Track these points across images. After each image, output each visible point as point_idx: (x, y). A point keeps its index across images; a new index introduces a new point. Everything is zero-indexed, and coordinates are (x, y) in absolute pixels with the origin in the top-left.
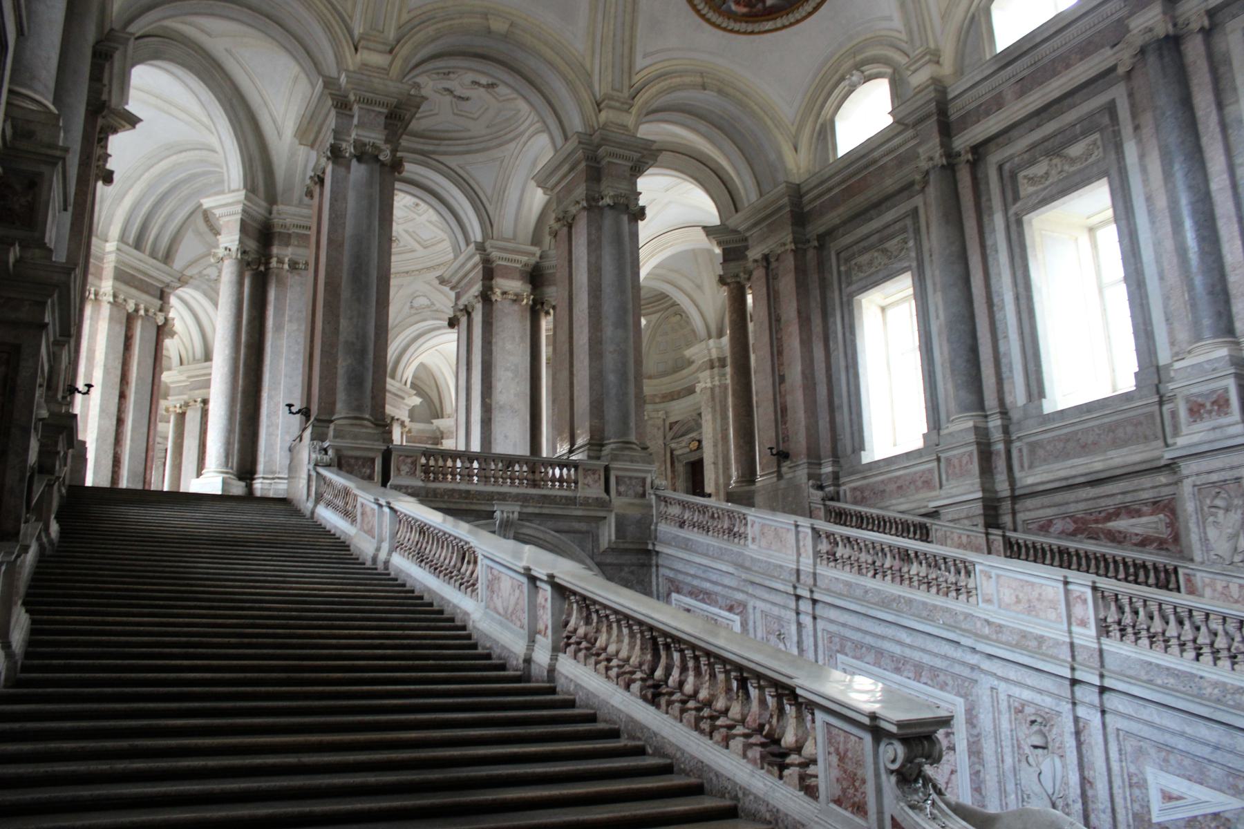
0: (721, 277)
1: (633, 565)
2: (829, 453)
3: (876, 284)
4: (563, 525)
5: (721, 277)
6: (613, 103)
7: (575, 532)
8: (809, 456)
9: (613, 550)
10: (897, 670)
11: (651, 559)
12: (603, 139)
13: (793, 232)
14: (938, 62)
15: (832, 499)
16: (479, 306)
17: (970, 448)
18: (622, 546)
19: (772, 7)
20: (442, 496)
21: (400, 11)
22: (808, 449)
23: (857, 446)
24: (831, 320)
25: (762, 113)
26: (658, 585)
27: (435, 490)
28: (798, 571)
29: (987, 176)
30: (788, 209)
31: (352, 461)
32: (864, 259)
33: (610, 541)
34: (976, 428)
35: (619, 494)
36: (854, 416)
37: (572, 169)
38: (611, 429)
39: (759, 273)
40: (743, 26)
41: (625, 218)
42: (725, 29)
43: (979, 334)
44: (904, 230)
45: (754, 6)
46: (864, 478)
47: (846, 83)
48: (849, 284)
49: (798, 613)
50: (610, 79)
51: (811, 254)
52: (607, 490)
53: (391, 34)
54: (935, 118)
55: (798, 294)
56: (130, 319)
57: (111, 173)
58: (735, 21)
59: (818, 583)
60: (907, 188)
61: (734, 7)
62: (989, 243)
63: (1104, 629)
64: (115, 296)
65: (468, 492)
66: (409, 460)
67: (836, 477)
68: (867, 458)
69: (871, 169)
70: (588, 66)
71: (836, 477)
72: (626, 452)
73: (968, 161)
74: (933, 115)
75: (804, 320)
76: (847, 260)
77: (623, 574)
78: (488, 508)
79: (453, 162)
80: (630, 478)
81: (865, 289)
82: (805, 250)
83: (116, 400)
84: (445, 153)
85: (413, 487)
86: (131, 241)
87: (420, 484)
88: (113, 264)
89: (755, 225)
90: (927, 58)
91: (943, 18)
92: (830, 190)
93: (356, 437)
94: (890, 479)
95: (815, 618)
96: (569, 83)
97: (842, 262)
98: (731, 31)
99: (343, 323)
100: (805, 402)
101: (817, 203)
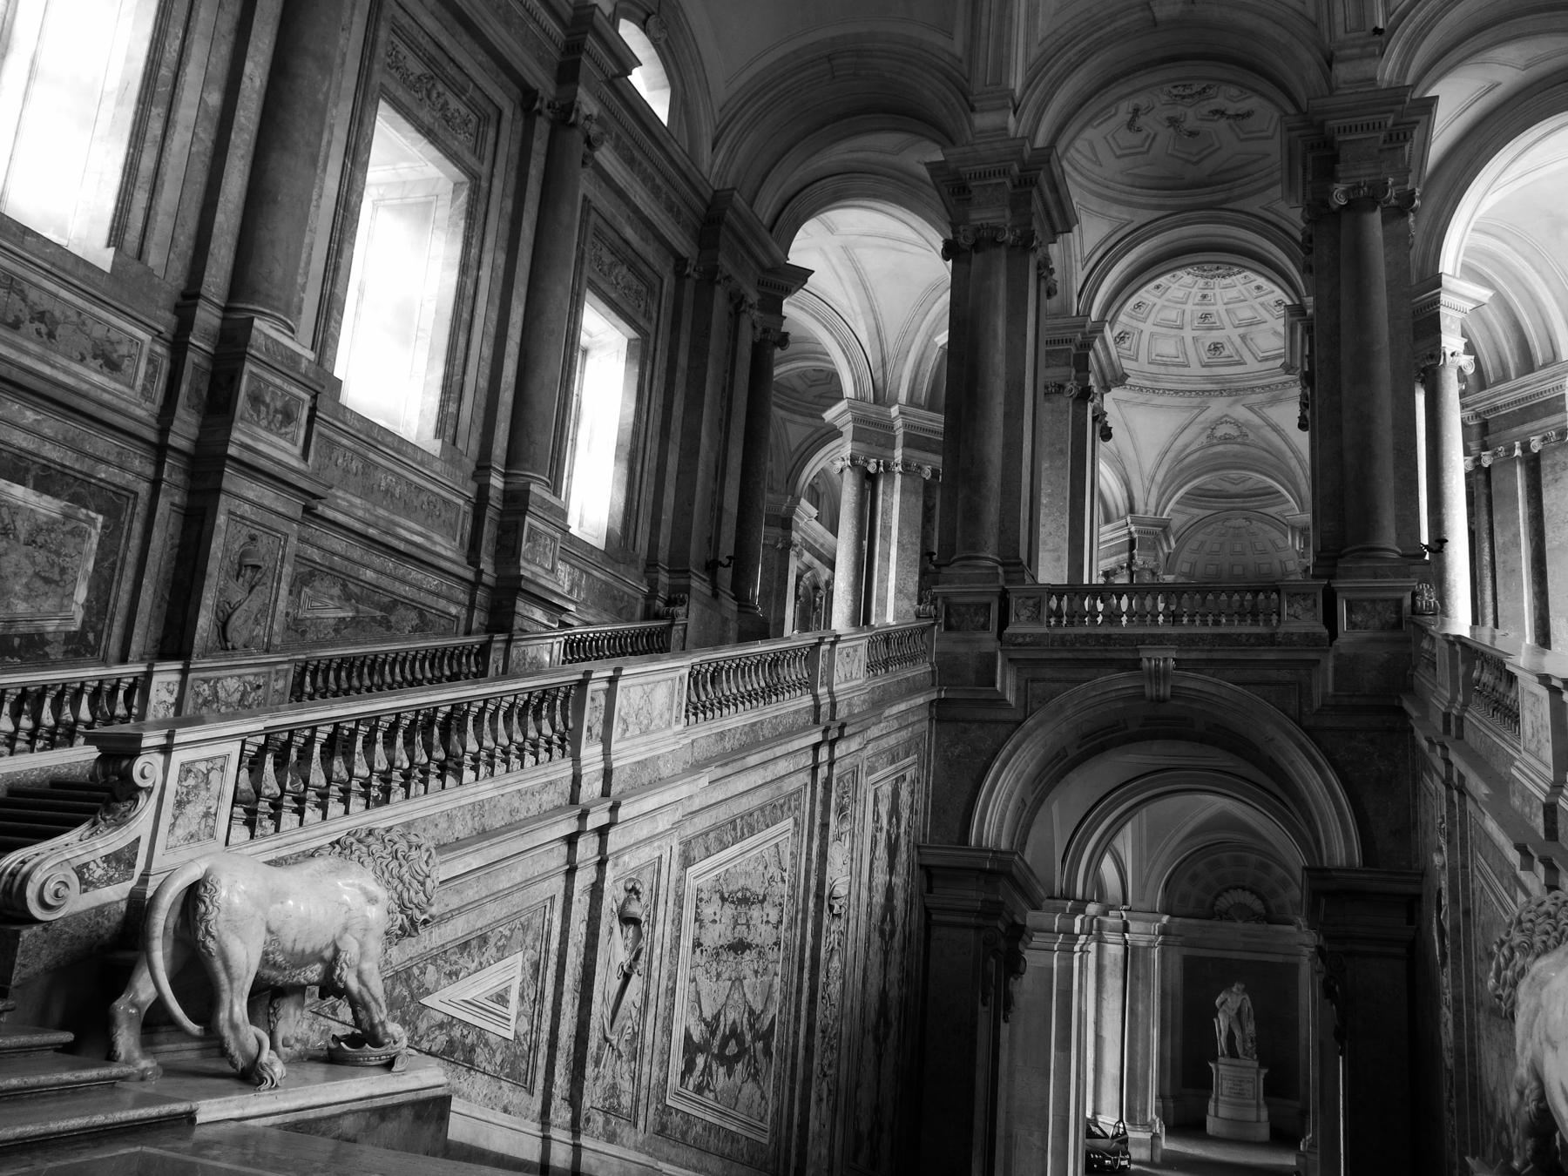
6: (1348, 52)
20: (1073, 644)
21: (1027, 45)
27: (1063, 637)
28: (1447, 716)
31: (963, 609)
35: (1352, 625)
37: (1305, 168)
41: (1376, 217)
49: (1449, 787)
53: (1017, 82)
56: (928, 487)
57: (787, 334)
64: (906, 464)
66: (1031, 602)
70: (1311, 13)
72: (1366, 564)
79: (1254, 205)
80: (1373, 601)
84: (1241, 197)
86: (922, 401)
87: (1044, 630)
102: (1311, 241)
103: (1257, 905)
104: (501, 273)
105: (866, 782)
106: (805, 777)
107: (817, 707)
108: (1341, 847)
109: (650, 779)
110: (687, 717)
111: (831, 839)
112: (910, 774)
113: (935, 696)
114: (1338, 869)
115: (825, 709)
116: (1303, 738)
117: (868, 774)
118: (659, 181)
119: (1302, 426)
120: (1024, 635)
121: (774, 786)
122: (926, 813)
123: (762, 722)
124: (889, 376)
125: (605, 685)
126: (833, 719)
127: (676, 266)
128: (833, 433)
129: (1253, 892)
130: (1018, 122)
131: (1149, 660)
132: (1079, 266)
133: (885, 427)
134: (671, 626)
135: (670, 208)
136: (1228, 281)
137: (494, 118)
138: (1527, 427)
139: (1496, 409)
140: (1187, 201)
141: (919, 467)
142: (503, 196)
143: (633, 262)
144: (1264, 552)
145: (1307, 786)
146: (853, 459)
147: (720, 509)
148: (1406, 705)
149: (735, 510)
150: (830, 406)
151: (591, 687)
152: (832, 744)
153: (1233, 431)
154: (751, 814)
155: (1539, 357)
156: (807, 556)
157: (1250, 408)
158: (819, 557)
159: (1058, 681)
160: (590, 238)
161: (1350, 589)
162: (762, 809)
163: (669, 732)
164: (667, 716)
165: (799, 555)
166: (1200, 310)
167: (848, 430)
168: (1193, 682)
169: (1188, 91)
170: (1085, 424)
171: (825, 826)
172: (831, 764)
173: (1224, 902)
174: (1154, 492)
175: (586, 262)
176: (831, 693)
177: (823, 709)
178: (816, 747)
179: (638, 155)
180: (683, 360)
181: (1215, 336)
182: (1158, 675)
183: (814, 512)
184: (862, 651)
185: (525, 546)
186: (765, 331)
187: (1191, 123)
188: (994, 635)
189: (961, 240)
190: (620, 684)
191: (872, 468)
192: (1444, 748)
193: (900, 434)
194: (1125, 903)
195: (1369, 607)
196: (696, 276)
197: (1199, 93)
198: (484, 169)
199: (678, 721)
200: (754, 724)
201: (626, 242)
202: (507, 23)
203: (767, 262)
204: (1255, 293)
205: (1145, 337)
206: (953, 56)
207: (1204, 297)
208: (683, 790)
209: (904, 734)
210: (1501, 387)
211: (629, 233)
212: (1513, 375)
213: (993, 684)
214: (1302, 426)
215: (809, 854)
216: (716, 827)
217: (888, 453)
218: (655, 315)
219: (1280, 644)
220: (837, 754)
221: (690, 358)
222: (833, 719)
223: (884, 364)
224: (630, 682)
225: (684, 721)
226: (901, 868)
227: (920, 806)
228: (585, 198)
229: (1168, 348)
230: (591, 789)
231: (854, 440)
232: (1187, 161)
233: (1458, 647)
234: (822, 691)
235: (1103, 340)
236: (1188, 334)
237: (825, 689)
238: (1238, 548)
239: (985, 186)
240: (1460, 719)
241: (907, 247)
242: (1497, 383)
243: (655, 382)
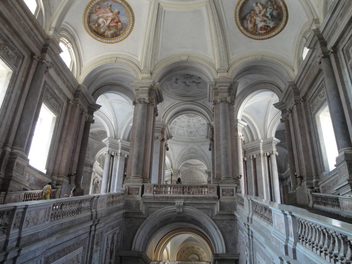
0: (281, 119)
1: (228, 220)
2: (315, 175)
3: (319, 108)
4: (200, 207)
5: (281, 119)
6: (221, 71)
7: (205, 209)
8: (307, 176)
9: (220, 214)
10: (264, 259)
11: (235, 218)
12: (215, 82)
13: (295, 98)
14: (319, 23)
15: (316, 192)
16: (211, 142)
17: (344, 163)
18: (222, 213)
19: (273, 27)
22: (307, 173)
23: (322, 170)
24: (311, 125)
25: (279, 62)
26: (237, 227)
27: (157, 198)
28: (248, 218)
29: (340, 55)
30: (292, 91)
32: (316, 100)
33: (217, 211)
34: (345, 154)
35: (223, 195)
36: (320, 158)
38: (223, 173)
39: (290, 115)
40: (265, 37)
41: (227, 105)
42: (259, 39)
43: (346, 116)
44: (323, 87)
45: (267, 29)
46: (324, 182)
47: (302, 43)
48: (313, 111)
49: (249, 235)
50: (220, 64)
51: (302, 103)
52: (218, 193)
54: (319, 42)
55: (298, 118)
56: (126, 160)
57: (94, 120)
58: (262, 36)
59: (253, 222)
60: (320, 71)
61: (260, 32)
62: (345, 80)
63: (299, 238)
64: (121, 154)
65: (168, 197)
66: (149, 188)
67: (317, 182)
68: (324, 174)
69: (311, 68)
71: (317, 182)
73: (332, 52)
74: (319, 40)
75: (302, 127)
76: (312, 102)
77: (224, 223)
78: (174, 202)
80: (228, 189)
81: (317, 111)
82: (300, 103)
83: (122, 181)
85: (149, 196)
86: (126, 139)
87: (152, 195)
88: (121, 146)
89: (287, 99)
90: (314, 22)
91: (318, 7)
92: (303, 80)
93: (134, 182)
94: (331, 181)
95: (252, 237)
96: (208, 69)
97: (310, 104)
98: (262, 39)
99: (134, 149)
100: (304, 157)
101: (301, 86)
102: (214, 109)
103: (197, 258)
104: (18, 96)
105: (105, 235)
106: (87, 235)
107: (92, 215)
108: (221, 248)
109: (35, 239)
110: (51, 219)
111: (94, 252)
112: (117, 232)
113: (124, 211)
114: (220, 254)
115: (94, 216)
116: (213, 222)
117: (105, 233)
118: (65, 80)
119: (210, 150)
120: (147, 196)
121: (77, 238)
122: (121, 242)
123: (75, 220)
124: (118, 133)
125: (22, 210)
126: (96, 218)
127: (68, 101)
128: (104, 146)
129: (196, 254)
130: (152, 77)
131: (177, 203)
132: (163, 111)
133: (117, 144)
134: (57, 191)
135: (67, 87)
136: (194, 118)
137: (22, 58)
138: (253, 153)
139: (247, 148)
140: (186, 99)
141: (124, 154)
142: (22, 76)
143: (56, 99)
144: (199, 178)
145: (213, 234)
146: (108, 152)
147: (73, 161)
148: (235, 214)
149: (77, 162)
150: (103, 139)
151: (17, 211)
152: (96, 225)
153: (193, 150)
154: (70, 247)
155: (255, 139)
156: (96, 175)
157: (198, 146)
158: (99, 175)
159: (156, 208)
160: (45, 91)
161: (223, 187)
162: (73, 245)
163: (44, 224)
164: (43, 219)
165: (94, 174)
166: (188, 124)
167: (108, 144)
168: (187, 208)
169: (188, 76)
170: (163, 146)
171: (92, 248)
172: (95, 230)
173: (190, 257)
174: (177, 163)
175: (43, 96)
176: (96, 211)
177: (93, 216)
178: (91, 226)
179: (60, 73)
180: (67, 123)
181: (191, 130)
182: (179, 207)
183: (99, 164)
184: (106, 199)
185: (15, 168)
186: (89, 119)
187: (188, 83)
188: (140, 196)
189: (137, 101)
190: (28, 210)
191: (113, 154)
192: (248, 226)
193: (120, 146)
194: (168, 259)
195: (227, 191)
196: (73, 104)
197: (190, 77)
198: (17, 69)
199: (47, 220)
200: (72, 221)
201: (55, 93)
202: (29, 36)
203: (91, 103)
204: (200, 121)
205: (176, 129)
206: (138, 61)
207: (189, 121)
208: (46, 242)
209: (116, 221)
210: (248, 144)
211: (56, 91)
212: (250, 142)
213: (139, 208)
214: (210, 150)
215: (87, 256)
216: (59, 252)
217: (117, 151)
218: (60, 112)
219: (207, 199)
220: (97, 228)
221: (69, 123)
222: (96, 218)
223: (117, 130)
224: (31, 209)
225: (49, 220)
226: (113, 257)
227: (119, 240)
228: (45, 81)
229: (181, 132)
230: (12, 244)
231: (109, 147)
232: (187, 91)
233: (250, 201)
234: (94, 210)
235: (168, 128)
236: (185, 129)
237: (95, 210)
238: (194, 177)
239: (143, 90)
240: (251, 219)
241: (124, 103)
242: (247, 143)
243: (59, 128)
